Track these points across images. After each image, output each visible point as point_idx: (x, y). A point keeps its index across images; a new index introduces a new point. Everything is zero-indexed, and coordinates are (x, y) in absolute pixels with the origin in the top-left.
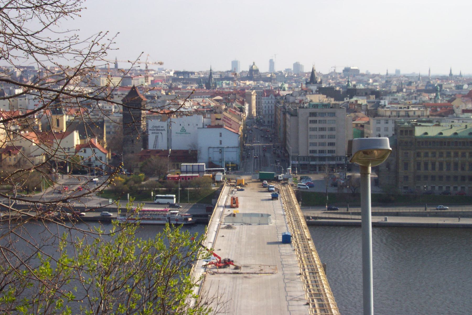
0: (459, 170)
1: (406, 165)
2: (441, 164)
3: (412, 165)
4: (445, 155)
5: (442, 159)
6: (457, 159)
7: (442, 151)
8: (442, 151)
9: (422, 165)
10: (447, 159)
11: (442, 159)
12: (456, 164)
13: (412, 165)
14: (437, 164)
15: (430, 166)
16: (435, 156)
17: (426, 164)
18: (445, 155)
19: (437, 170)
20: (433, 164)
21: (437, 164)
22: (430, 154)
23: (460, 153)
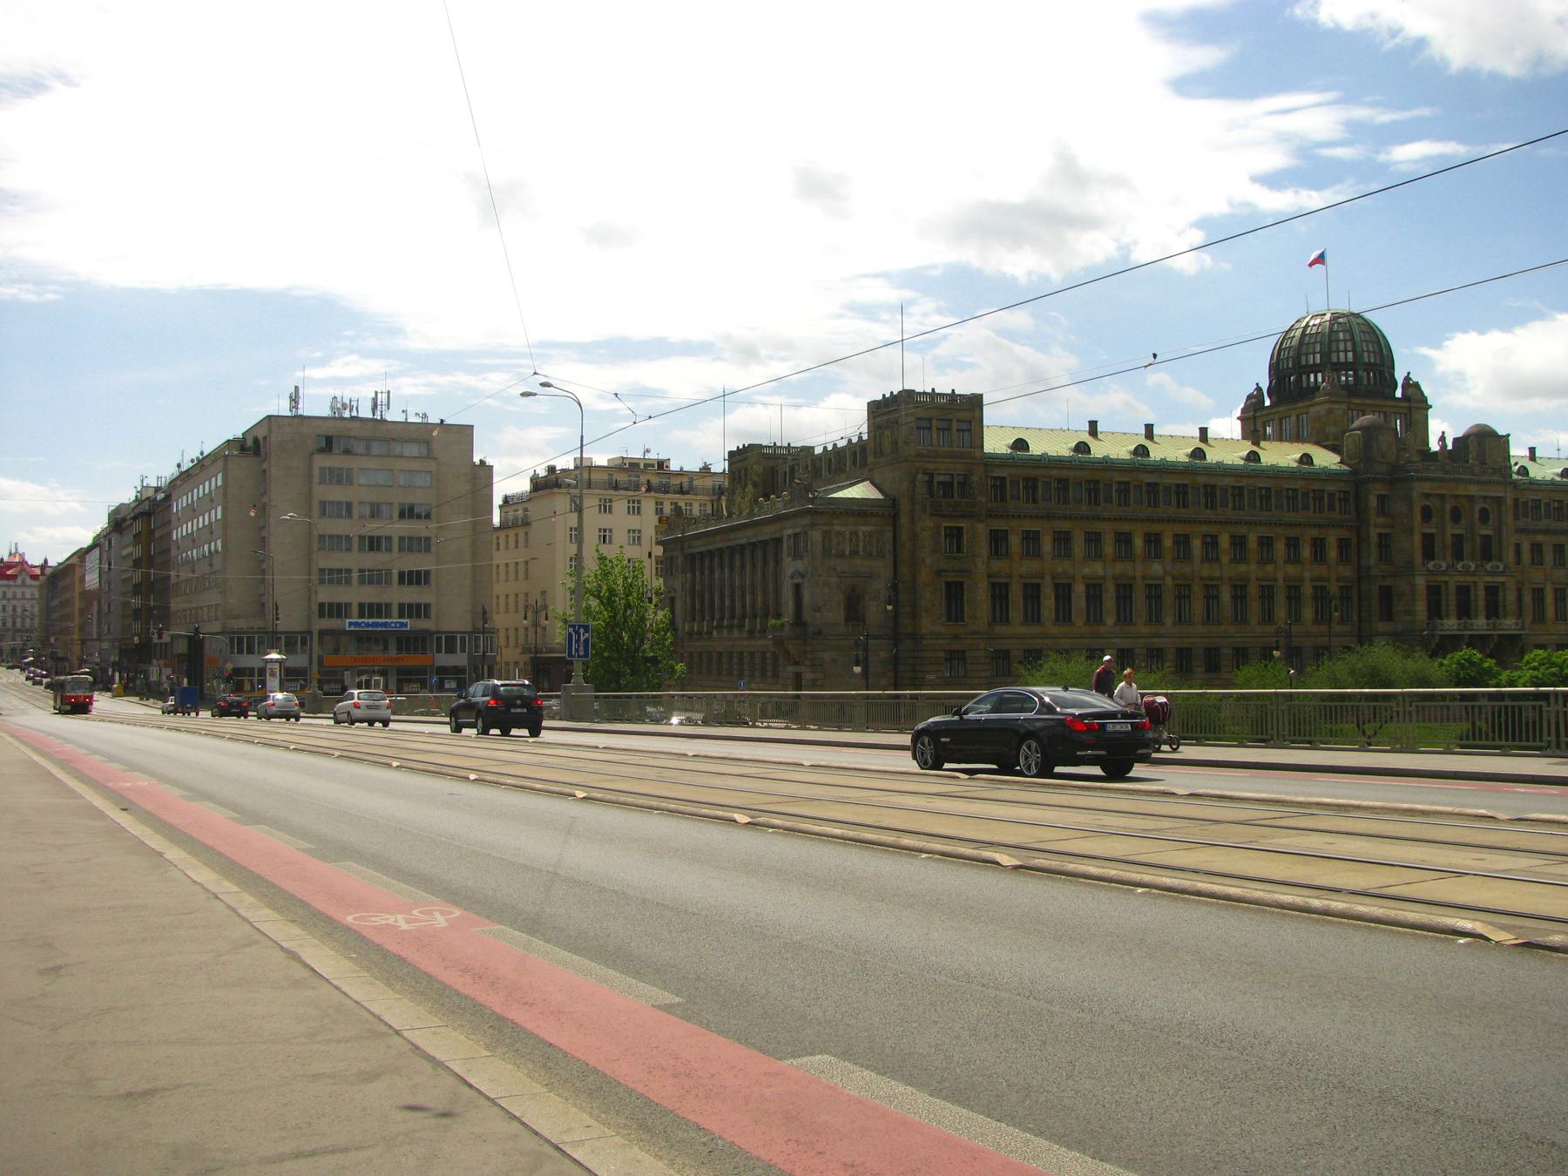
0: (1169, 620)
1: (955, 593)
2: (1094, 592)
3: (979, 597)
4: (1109, 549)
5: (1097, 569)
6: (1157, 568)
7: (1098, 526)
8: (1098, 526)
9: (1016, 595)
10: (1119, 568)
11: (1097, 569)
12: (1154, 593)
13: (979, 597)
14: (1079, 589)
15: (1048, 604)
16: (1068, 554)
17: (1032, 593)
18: (1109, 549)
19: (1078, 618)
20: (1063, 593)
21: (1079, 589)
22: (1047, 545)
23: (1168, 542)
